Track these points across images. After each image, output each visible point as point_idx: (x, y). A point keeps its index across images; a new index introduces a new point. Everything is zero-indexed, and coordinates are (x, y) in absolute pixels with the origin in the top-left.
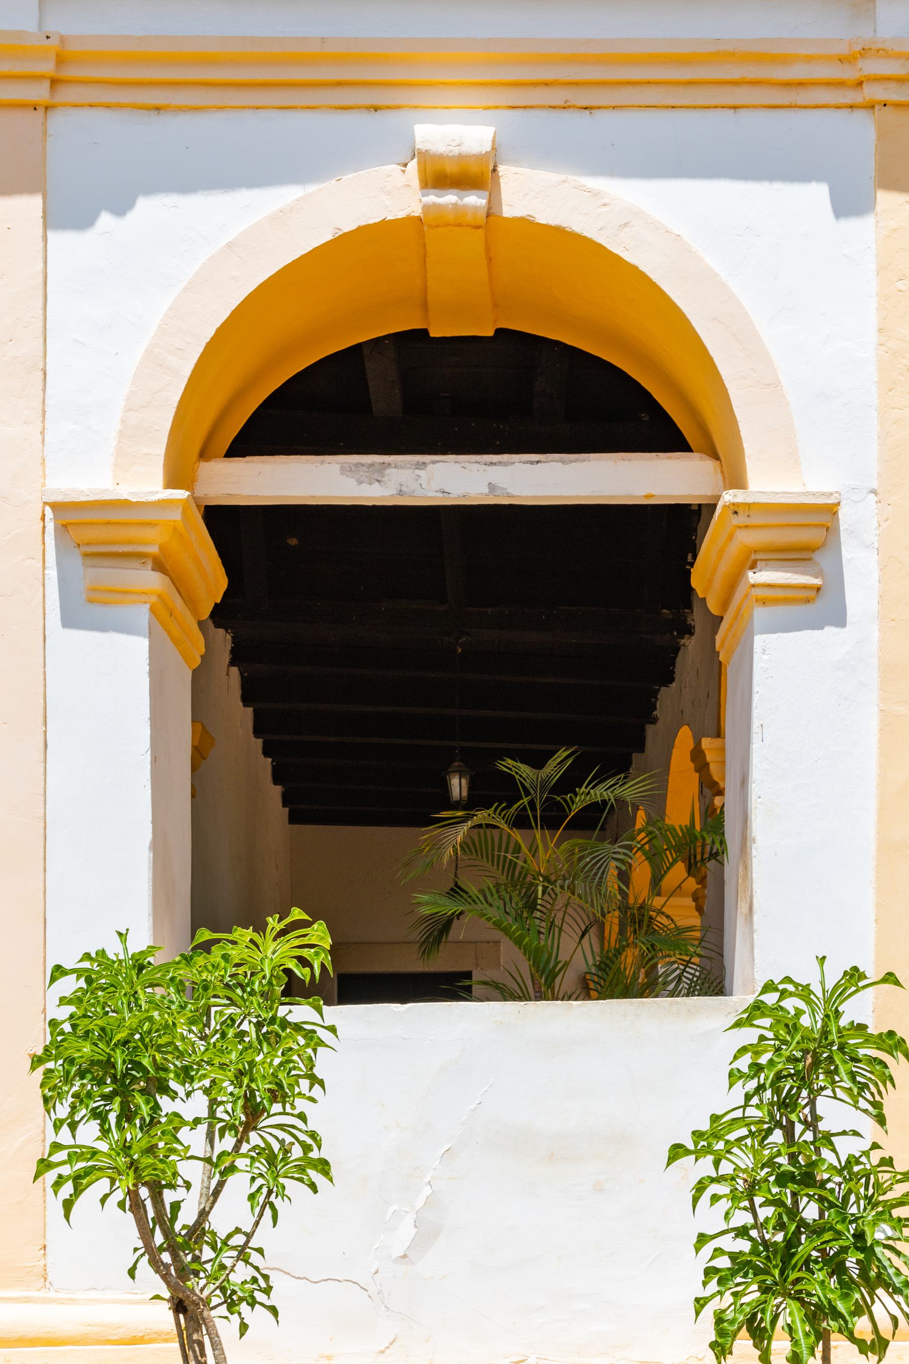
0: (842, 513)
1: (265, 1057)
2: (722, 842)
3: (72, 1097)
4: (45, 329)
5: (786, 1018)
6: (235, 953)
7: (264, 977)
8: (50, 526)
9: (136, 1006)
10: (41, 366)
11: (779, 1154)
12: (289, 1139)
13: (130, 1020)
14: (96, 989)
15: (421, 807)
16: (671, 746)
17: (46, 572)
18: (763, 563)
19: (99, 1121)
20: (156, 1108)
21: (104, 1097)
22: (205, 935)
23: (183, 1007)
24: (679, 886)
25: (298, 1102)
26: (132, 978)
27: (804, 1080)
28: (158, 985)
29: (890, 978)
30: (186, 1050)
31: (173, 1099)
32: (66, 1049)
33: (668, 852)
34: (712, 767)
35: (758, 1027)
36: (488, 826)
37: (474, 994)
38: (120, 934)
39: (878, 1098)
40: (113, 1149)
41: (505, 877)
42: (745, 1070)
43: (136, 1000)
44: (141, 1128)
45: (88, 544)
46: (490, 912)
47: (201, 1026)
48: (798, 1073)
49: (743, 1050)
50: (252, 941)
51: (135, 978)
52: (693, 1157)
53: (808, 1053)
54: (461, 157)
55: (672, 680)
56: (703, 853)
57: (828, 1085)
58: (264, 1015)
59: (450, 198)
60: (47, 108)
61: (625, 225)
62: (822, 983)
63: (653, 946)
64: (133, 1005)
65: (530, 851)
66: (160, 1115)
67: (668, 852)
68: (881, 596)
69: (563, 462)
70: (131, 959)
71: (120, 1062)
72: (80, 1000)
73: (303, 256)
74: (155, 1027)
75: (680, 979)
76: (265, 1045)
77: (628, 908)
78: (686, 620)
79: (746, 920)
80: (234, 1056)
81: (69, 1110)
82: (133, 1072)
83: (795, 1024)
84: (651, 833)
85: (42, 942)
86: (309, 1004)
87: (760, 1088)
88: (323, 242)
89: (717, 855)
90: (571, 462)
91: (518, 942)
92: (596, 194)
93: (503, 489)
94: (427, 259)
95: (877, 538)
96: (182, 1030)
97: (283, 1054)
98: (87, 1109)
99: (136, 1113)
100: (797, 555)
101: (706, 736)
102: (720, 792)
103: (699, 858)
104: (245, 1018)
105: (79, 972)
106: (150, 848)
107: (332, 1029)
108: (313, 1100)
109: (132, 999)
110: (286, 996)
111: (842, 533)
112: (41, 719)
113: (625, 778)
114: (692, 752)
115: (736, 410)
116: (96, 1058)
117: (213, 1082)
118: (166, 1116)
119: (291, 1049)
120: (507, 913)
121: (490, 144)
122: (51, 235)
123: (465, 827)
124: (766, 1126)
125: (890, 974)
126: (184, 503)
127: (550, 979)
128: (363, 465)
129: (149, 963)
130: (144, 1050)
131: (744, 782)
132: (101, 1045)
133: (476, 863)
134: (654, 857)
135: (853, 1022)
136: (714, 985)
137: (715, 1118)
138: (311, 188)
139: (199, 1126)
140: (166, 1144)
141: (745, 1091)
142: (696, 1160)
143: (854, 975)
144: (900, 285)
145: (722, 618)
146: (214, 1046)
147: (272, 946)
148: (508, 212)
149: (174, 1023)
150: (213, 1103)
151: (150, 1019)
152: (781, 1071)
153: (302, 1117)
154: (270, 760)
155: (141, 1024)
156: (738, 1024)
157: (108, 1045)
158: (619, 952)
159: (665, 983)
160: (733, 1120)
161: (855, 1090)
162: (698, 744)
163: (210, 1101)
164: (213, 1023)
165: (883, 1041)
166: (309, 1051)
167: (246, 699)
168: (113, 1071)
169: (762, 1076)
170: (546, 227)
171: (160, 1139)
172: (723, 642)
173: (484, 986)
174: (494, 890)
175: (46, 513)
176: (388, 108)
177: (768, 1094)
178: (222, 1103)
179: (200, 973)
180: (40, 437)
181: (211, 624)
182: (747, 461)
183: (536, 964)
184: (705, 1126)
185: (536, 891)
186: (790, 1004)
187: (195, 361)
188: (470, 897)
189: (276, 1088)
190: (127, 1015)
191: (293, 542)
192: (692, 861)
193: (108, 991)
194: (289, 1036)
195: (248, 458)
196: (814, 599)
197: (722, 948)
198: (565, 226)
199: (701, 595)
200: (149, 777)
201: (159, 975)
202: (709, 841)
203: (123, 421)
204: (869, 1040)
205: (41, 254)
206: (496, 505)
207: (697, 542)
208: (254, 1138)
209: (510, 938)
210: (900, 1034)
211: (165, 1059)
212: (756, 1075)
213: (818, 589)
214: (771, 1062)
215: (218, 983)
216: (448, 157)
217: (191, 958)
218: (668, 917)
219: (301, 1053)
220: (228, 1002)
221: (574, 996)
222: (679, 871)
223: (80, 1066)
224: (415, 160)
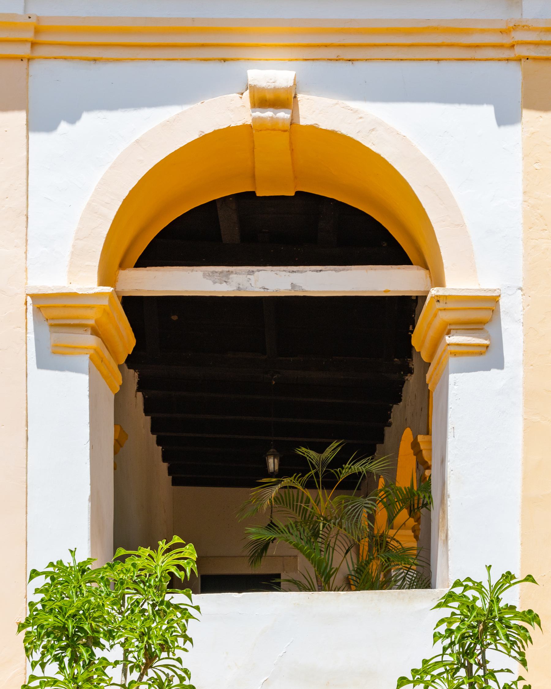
0: (502, 302)
1: (157, 625)
2: (430, 497)
3: (43, 648)
4: (28, 191)
5: (467, 602)
6: (139, 563)
7: (157, 577)
8: (30, 308)
9: (80, 594)
11: (463, 683)
12: (171, 673)
13: (77, 602)
14: (57, 584)
15: (250, 475)
16: (399, 440)
17: (28, 335)
19: (58, 663)
20: (92, 654)
21: (61, 648)
22: (122, 552)
23: (108, 595)
24: (404, 524)
25: (177, 651)
26: (78, 577)
27: (478, 639)
28: (93, 581)
29: (529, 578)
30: (110, 620)
31: (102, 649)
32: (39, 619)
33: (397, 503)
34: (424, 452)
35: (451, 607)
36: (291, 487)
37: (282, 587)
38: (71, 551)
39: (522, 650)
40: (67, 679)
41: (300, 517)
42: (443, 633)
43: (81, 590)
44: (83, 667)
45: (52, 319)
46: (291, 538)
47: (119, 606)
48: (474, 635)
49: (442, 621)
50: (149, 555)
51: (80, 577)
52: (412, 684)
53: (481, 623)
54: (275, 89)
55: (400, 400)
56: (418, 504)
57: (492, 642)
58: (157, 599)
59: (268, 114)
60: (29, 60)
61: (373, 130)
62: (489, 581)
63: (388, 559)
64: (79, 593)
65: (315, 502)
66: (94, 659)
67: (397, 503)
68: (524, 351)
69: (335, 271)
70: (78, 566)
71: (71, 627)
72: (47, 590)
73: (181, 148)
74: (92, 607)
75: (404, 579)
76: (157, 617)
77: (373, 536)
78: (408, 365)
79: (444, 544)
80: (138, 624)
81: (40, 656)
82: (79, 633)
83: (473, 606)
84: (387, 491)
85: (25, 555)
86: (183, 593)
87: (452, 644)
89: (427, 505)
90: (340, 271)
91: (308, 556)
92: (356, 111)
93: (300, 287)
94: (255, 150)
95: (522, 316)
96: (108, 608)
97: (168, 623)
98: (51, 655)
99: (80, 658)
100: (475, 326)
101: (420, 434)
102: (429, 468)
103: (416, 506)
104: (145, 601)
105: (46, 574)
106: (89, 500)
107: (197, 608)
108: (186, 650)
109: (78, 590)
110: (170, 588)
111: (501, 314)
112: (25, 423)
113: (372, 459)
114: (412, 443)
116: (56, 625)
117: (126, 639)
118: (98, 659)
119: (173, 620)
120: (302, 539)
121: (293, 81)
122: (31, 135)
123: (277, 488)
124: (455, 666)
125: (530, 576)
126: (110, 295)
127: (327, 579)
128: (216, 272)
129: (88, 568)
130: (85, 620)
131: (443, 461)
132: (59, 617)
133: (283, 509)
134: (389, 506)
135: (507, 604)
136: (425, 582)
137: (425, 662)
138: (186, 108)
139: (118, 665)
140: (98, 676)
141: (443, 646)
142: (414, 686)
143: (508, 576)
144: (536, 166)
145: (430, 364)
146: (127, 618)
147: (162, 558)
148: (303, 122)
149: (103, 604)
150: (126, 652)
151: (89, 602)
152: (465, 633)
153: (179, 660)
154: (161, 447)
155: (83, 605)
156: (439, 606)
157: (64, 617)
158: (368, 563)
159: (396, 581)
160: (436, 662)
161: (509, 645)
162: (416, 439)
163: (125, 651)
164: (126, 604)
165: (525, 616)
166: (184, 621)
167: (147, 411)
168: (66, 633)
169: (453, 636)
171: (95, 673)
172: (431, 378)
173: (287, 583)
174: (294, 525)
175: (28, 300)
176: (232, 60)
177: (457, 647)
178: (131, 652)
179: (118, 574)
180: (24, 255)
181: (126, 367)
182: (445, 270)
183: (319, 569)
184: (419, 666)
185: (319, 526)
186: (470, 594)
187: (117, 210)
188: (280, 529)
189: (164, 643)
190: (75, 599)
191: (175, 318)
192: (412, 509)
193: (64, 585)
194: (172, 612)
195: (148, 268)
196: (484, 353)
197: (429, 560)
198: (337, 130)
199: (417, 350)
200: (89, 457)
201: (94, 576)
202: (422, 496)
203: (74, 246)
204: (517, 615)
205: (25, 146)
206: (295, 296)
207: (415, 318)
208: (151, 673)
209: (304, 554)
210: (535, 611)
211: (98, 626)
212: (450, 636)
213: (487, 347)
214: (459, 628)
215: (130, 581)
216: (267, 89)
217: (114, 565)
218: (397, 541)
219: (179, 622)
220: (135, 592)
221: (342, 589)
222: (405, 513)
223: (47, 629)
224: (248, 91)
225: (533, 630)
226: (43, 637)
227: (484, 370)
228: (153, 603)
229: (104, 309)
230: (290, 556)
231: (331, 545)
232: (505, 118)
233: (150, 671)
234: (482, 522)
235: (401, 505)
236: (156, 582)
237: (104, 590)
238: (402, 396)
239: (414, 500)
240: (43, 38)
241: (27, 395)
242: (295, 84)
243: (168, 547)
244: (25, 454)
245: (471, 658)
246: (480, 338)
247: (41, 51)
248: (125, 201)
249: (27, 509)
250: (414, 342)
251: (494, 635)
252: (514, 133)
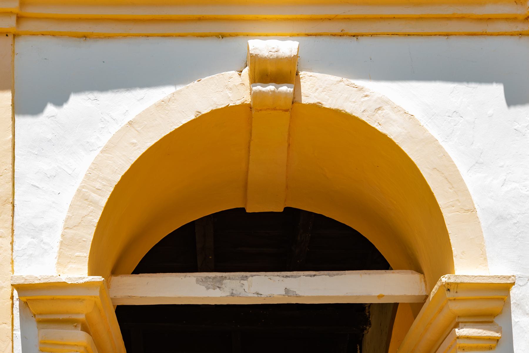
0: (514, 292)
4: (14, 177)
8: (17, 304)
10: (11, 200)
17: (14, 332)
18: (463, 324)
45: (40, 314)
61: (379, 109)
88: (189, 120)
92: (361, 89)
100: (484, 319)
115: (447, 226)
148: (305, 100)
170: (329, 110)
175: (14, 295)
176: (230, 36)
180: (10, 246)
182: (454, 258)
187: (108, 197)
196: (494, 347)
198: (341, 109)
203: (63, 235)
205: (10, 129)
213: (497, 340)
224: (248, 68)
240: (30, 11)
246: (491, 331)
247: (28, 26)
248: (117, 187)
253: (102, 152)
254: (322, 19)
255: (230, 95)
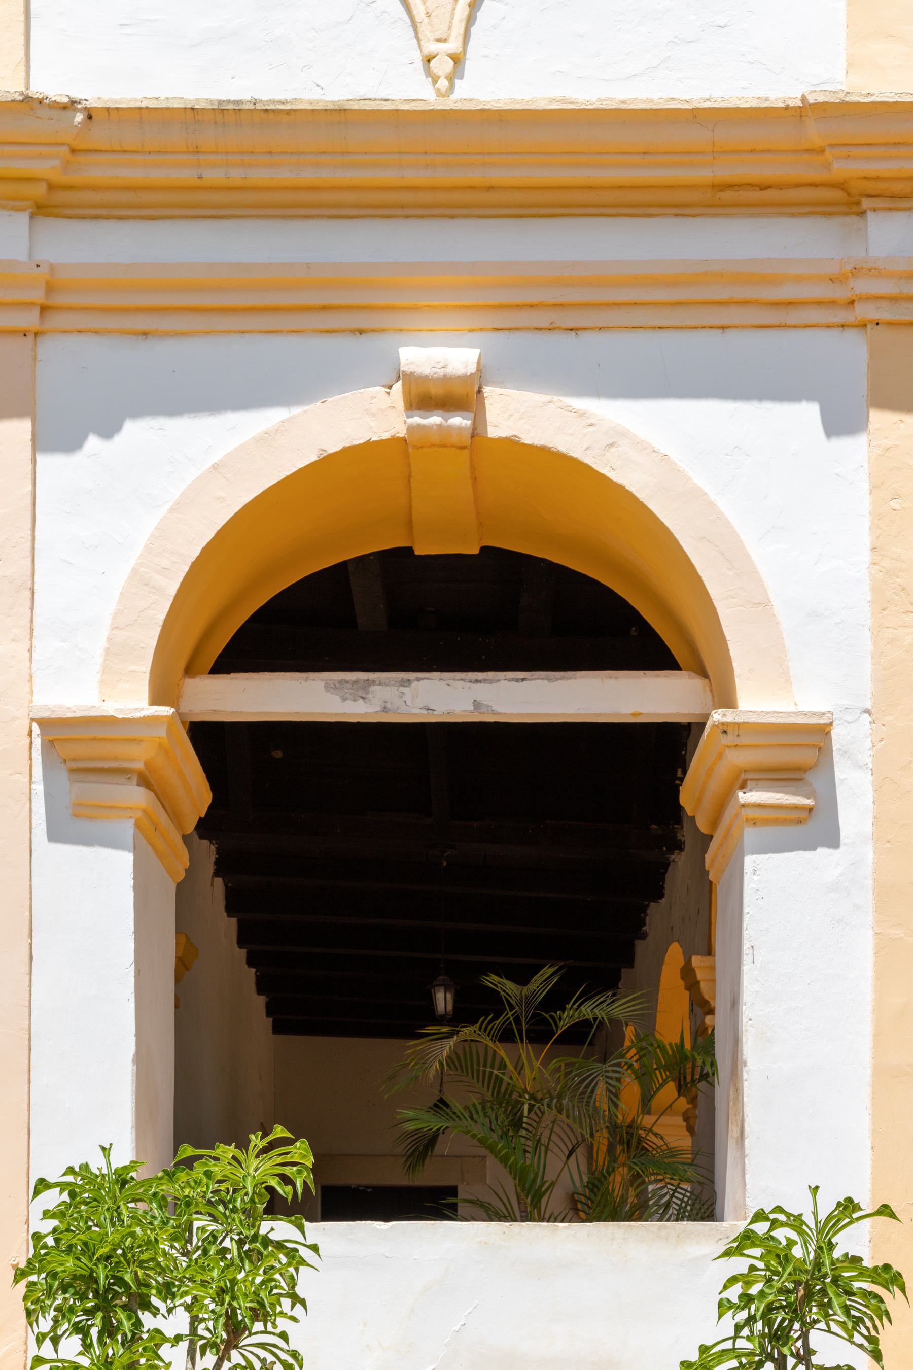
0: (836, 733)
1: (247, 1276)
2: (713, 1064)
3: (55, 1310)
5: (777, 1248)
6: (217, 1170)
7: (246, 1194)
8: (37, 742)
9: (119, 1221)
10: (29, 584)
12: (270, 1358)
14: (80, 1203)
16: (660, 962)
17: (33, 787)
19: (80, 1336)
20: (138, 1324)
21: (86, 1312)
22: (188, 1151)
23: (165, 1223)
24: (670, 1106)
25: (280, 1321)
27: (796, 1312)
28: (140, 1200)
29: (885, 1210)
31: (155, 1315)
32: (49, 1263)
34: (703, 986)
35: (748, 1256)
38: (103, 1149)
39: (873, 1333)
40: (95, 1365)
41: (490, 1093)
42: (735, 1300)
43: (119, 1214)
44: (123, 1344)
45: (74, 760)
47: (183, 1242)
48: (789, 1305)
49: (733, 1280)
50: (234, 1158)
51: (118, 1193)
53: (800, 1285)
54: (446, 379)
55: (661, 896)
58: (246, 1232)
61: (612, 445)
62: (815, 1213)
65: (515, 1068)
66: (142, 1332)
67: (657, 1072)
68: (875, 817)
69: (549, 680)
71: (102, 1277)
73: (288, 477)
74: (138, 1242)
78: (675, 836)
80: (215, 1274)
81: (51, 1323)
82: (115, 1288)
83: (786, 1255)
84: (642, 1049)
85: (26, 1152)
86: (291, 1222)
87: (751, 1320)
88: (308, 463)
89: (708, 1077)
90: (557, 680)
91: (504, 1160)
92: (582, 414)
93: (488, 706)
94: (412, 480)
95: (871, 759)
96: (164, 1246)
97: (265, 1273)
99: (118, 1328)
101: (697, 954)
102: (711, 1011)
103: (689, 1079)
104: (226, 1235)
105: (62, 1186)
106: (133, 1061)
107: (315, 1248)
108: (294, 1319)
109: (115, 1214)
111: (834, 754)
113: (613, 995)
114: (682, 969)
115: (724, 629)
116: (78, 1273)
117: (195, 1298)
119: (273, 1267)
120: (493, 1131)
122: (40, 458)
123: (452, 1042)
124: (757, 1358)
125: (885, 1206)
127: (536, 1199)
128: (347, 682)
129: (132, 1178)
130: (126, 1266)
131: (735, 1003)
132: (83, 1259)
133: (464, 1079)
134: (643, 1076)
135: (847, 1254)
136: (706, 1206)
137: (704, 1349)
139: (180, 1343)
140: (147, 1360)
141: (734, 1322)
143: (848, 1206)
144: (894, 504)
145: (711, 837)
146: (196, 1262)
147: (254, 1163)
148: (493, 432)
149: (156, 1240)
150: (195, 1321)
151: (133, 1235)
152: (773, 1302)
153: (284, 1336)
155: (123, 1239)
156: (728, 1253)
157: (91, 1259)
160: (723, 1351)
161: (850, 1325)
162: (688, 962)
163: (192, 1318)
164: (195, 1239)
165: (879, 1275)
166: (291, 1270)
168: (95, 1286)
169: (753, 1307)
170: (532, 447)
171: (142, 1356)
172: (713, 861)
173: (468, 1204)
174: (479, 1107)
176: (373, 331)
177: (759, 1326)
178: (203, 1320)
179: (182, 1188)
180: (28, 655)
181: (196, 837)
182: (736, 680)
185: (521, 1109)
186: (782, 1234)
187: (181, 580)
188: (454, 1113)
189: (258, 1307)
190: (110, 1230)
192: (682, 1083)
193: (91, 1205)
195: (233, 675)
199: (690, 814)
200: (133, 990)
201: (141, 1191)
202: (700, 1062)
203: (109, 639)
204: (864, 1273)
205: (30, 476)
206: (480, 722)
207: (687, 758)
208: (236, 1357)
209: (496, 1157)
210: (896, 1267)
211: (147, 1275)
213: (811, 810)
214: (762, 1293)
215: (200, 1200)
216: (432, 379)
217: (174, 1174)
219: (283, 1271)
221: (560, 1218)
222: (671, 1087)
223: (63, 1280)
224: (400, 382)
225: (892, 1301)
226: (56, 1293)
227: (805, 850)
228: (240, 1239)
229: (160, 744)
230: (474, 1157)
231: (542, 1142)
232: (838, 424)
233: (234, 1353)
234: (801, 1115)
235: (664, 1077)
236: (245, 1203)
237: (157, 1215)
238: (664, 888)
239: (685, 1068)
241: (31, 886)
242: (479, 370)
243: (265, 1144)
244: (28, 984)
245: (784, 1344)
246: (798, 795)
247: (57, 320)
248: (194, 565)
249: (29, 1075)
250: (686, 798)
251: (825, 1307)
252: (854, 449)
253: (171, 510)
254: (519, 307)
255: (373, 424)
